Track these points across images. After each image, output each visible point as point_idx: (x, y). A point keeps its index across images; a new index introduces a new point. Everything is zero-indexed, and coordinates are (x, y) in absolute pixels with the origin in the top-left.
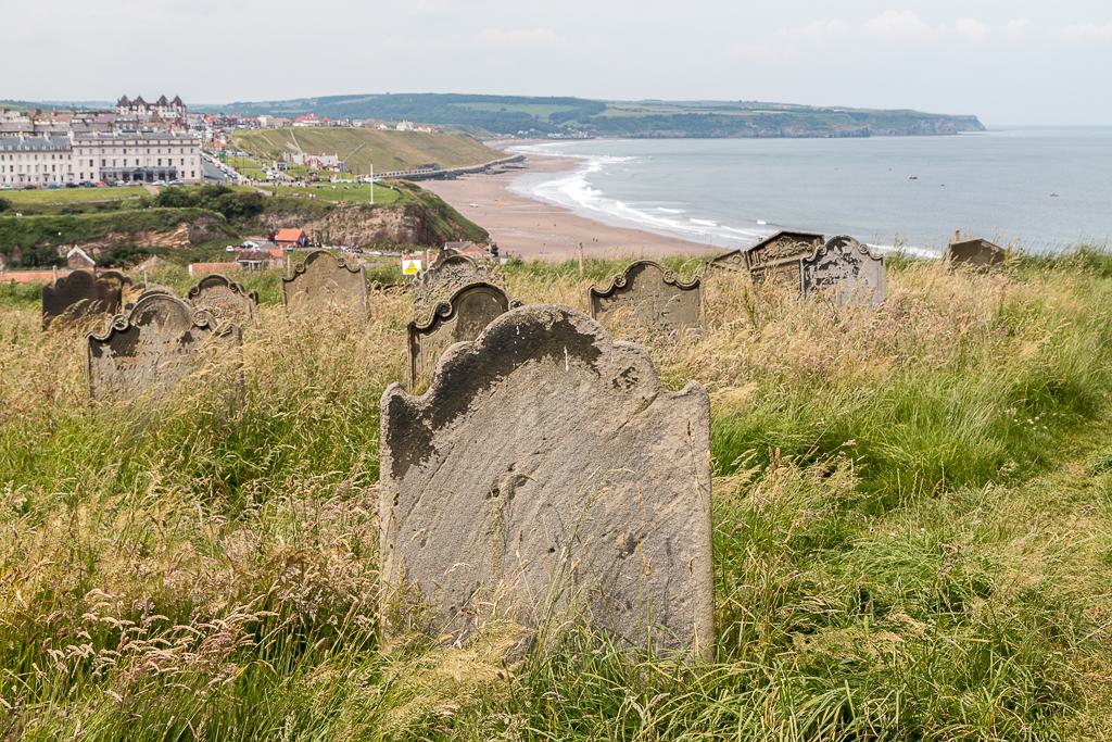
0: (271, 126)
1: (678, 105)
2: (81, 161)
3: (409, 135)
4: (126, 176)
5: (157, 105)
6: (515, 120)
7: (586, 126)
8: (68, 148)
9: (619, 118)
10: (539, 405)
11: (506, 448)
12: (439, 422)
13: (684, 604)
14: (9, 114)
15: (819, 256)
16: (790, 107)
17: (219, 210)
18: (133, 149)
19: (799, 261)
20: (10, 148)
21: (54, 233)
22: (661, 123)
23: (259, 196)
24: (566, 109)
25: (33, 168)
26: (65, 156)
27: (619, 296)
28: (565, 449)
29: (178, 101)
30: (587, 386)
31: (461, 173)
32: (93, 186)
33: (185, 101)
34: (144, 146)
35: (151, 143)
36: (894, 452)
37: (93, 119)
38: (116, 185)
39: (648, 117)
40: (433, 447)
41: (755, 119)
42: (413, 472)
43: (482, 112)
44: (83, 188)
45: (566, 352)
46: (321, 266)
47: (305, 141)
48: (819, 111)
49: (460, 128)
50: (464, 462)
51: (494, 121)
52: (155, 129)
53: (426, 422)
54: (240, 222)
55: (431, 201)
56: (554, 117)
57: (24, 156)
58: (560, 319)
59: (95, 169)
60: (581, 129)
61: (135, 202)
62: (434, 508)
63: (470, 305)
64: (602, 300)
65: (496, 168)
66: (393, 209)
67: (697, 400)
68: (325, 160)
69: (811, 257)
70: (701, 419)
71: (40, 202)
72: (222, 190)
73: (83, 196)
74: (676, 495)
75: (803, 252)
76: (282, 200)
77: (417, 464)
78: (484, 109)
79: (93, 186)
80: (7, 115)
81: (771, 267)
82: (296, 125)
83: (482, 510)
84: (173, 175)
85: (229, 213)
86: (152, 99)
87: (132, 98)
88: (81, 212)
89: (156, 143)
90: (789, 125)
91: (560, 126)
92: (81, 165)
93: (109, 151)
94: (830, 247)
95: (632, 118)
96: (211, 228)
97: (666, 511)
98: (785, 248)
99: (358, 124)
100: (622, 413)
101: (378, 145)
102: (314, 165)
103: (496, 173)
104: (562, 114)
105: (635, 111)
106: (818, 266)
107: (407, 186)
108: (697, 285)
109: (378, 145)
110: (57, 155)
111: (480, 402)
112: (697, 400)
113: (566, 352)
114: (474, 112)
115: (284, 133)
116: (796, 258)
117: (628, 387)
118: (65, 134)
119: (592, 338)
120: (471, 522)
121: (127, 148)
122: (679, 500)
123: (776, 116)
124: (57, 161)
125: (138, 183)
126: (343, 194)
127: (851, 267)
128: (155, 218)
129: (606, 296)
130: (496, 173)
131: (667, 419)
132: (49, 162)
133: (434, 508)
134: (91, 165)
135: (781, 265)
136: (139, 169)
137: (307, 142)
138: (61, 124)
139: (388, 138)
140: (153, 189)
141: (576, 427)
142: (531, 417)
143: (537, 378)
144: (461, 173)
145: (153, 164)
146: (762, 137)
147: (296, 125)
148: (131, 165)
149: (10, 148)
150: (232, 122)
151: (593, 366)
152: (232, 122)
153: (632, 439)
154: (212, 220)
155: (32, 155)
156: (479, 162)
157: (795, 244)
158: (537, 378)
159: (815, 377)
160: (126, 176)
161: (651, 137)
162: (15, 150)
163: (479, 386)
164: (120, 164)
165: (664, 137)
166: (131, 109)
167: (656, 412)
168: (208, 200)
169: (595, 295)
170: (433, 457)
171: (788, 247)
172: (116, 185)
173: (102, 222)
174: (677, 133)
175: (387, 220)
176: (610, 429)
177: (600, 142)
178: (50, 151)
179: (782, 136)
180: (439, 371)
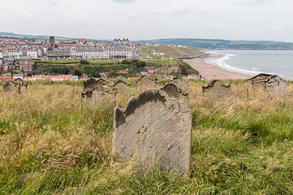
0: (149, 46)
1: (249, 42)
2: (105, 53)
3: (181, 48)
4: (115, 57)
5: (123, 41)
6: (207, 45)
7: (225, 47)
8: (102, 50)
9: (234, 45)
10: (151, 112)
11: (143, 122)
12: (127, 115)
13: (183, 163)
14: (90, 42)
15: (269, 80)
16: (279, 42)
17: (136, 65)
18: (117, 51)
19: (263, 82)
20: (90, 50)
21: (98, 70)
22: (244, 46)
23: (145, 62)
24: (220, 42)
25: (95, 55)
26: (102, 52)
27: (210, 88)
28: (156, 123)
29: (128, 40)
30: (163, 108)
31: (193, 58)
32: (107, 59)
33: (129, 40)
34: (119, 50)
35: (121, 49)
36: (274, 130)
37: (108, 44)
38: (113, 59)
39: (241, 44)
40: (125, 121)
41: (269, 45)
42: (121, 126)
43: (199, 43)
44: (105, 59)
45: (158, 100)
46: (145, 78)
47: (157, 49)
48: (287, 43)
49: (194, 47)
50: (132, 125)
51: (202, 45)
52: (122, 46)
53: (124, 115)
54: (140, 68)
55: (186, 64)
56: (218, 44)
57: (93, 52)
58: (157, 92)
59: (108, 55)
60: (224, 47)
61: (117, 63)
62: (125, 135)
63: (168, 89)
64: (205, 89)
65: (202, 57)
66: (176, 66)
67: (189, 113)
68: (161, 54)
69: (266, 80)
70: (190, 118)
71: (96, 62)
72: (137, 61)
73: (105, 61)
74: (183, 136)
75: (265, 79)
76: (150, 63)
77: (122, 125)
78: (200, 42)
79: (107, 59)
80: (90, 43)
81: (257, 82)
82: (154, 45)
83: (136, 136)
84: (125, 57)
85: (138, 66)
87: (117, 39)
88: (105, 65)
89: (122, 49)
90: (278, 47)
91: (219, 47)
92: (105, 54)
93: (111, 51)
94: (272, 78)
95: (237, 45)
96: (133, 69)
97: (180, 140)
98: (262, 78)
99: (169, 45)
100: (171, 115)
101: (174, 51)
102: (158, 55)
103: (202, 58)
104: (219, 44)
105: (238, 43)
106: (268, 83)
107: (180, 60)
108: (229, 86)
109: (174, 51)
110: (100, 52)
111: (137, 111)
112: (189, 113)
113: (158, 100)
114: (197, 43)
115: (151, 47)
116: (263, 81)
117: (172, 109)
118: (102, 47)
119: (164, 97)
120: (133, 139)
121: (116, 51)
122: (183, 137)
123: (275, 44)
124: (100, 53)
125: (117, 59)
126: (164, 62)
127: (277, 83)
128: (121, 67)
129: (206, 88)
130: (202, 58)
131: (181, 117)
132: (98, 54)
133: (125, 135)
134: (107, 54)
135: (259, 82)
137: (157, 49)
138: (101, 45)
139: (175, 49)
140: (121, 60)
141: (159, 118)
142: (149, 115)
143: (151, 106)
144: (193, 58)
145: (121, 54)
146: (271, 50)
147: (154, 45)
148: (116, 54)
149: (90, 50)
150: (140, 45)
151: (164, 104)
152: (140, 45)
153: (173, 122)
154: (134, 67)
155: (95, 52)
156: (198, 55)
157: (264, 77)
158: (151, 106)
159: (257, 111)
160: (115, 57)
161: (242, 49)
162: (91, 51)
163: (137, 107)
164: (114, 54)
165: (245, 50)
166: (117, 42)
167: (179, 115)
168: (133, 63)
169: (204, 88)
170: (125, 123)
171: (262, 78)
172: (113, 59)
173: (109, 67)
174: (248, 49)
175: (175, 68)
176: (167, 119)
177: (228, 50)
179: (277, 50)
180: (128, 103)
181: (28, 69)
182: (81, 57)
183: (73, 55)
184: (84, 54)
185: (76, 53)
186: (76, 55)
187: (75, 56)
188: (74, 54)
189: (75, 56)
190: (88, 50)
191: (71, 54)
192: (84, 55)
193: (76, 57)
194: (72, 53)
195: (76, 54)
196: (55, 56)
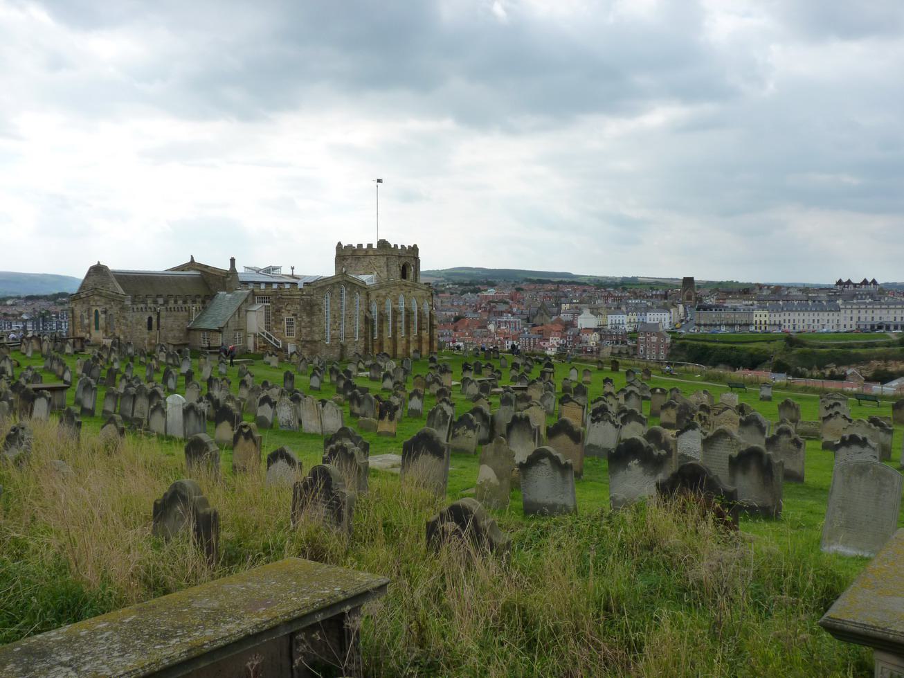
2: (845, 317)
5: (861, 284)
18: (878, 311)
29: (874, 282)
59: (854, 322)
86: (855, 281)
87: (844, 280)
132: (812, 317)
134: (851, 320)
136: (881, 323)
148: (877, 320)
178: (827, 311)
181: (658, 354)
182: (780, 325)
183: (758, 322)
184: (789, 320)
185: (768, 315)
186: (768, 322)
187: (765, 323)
188: (763, 319)
189: (765, 323)
190: (799, 309)
191: (755, 319)
192: (787, 321)
193: (766, 328)
194: (758, 316)
195: (766, 319)
196: (714, 323)
